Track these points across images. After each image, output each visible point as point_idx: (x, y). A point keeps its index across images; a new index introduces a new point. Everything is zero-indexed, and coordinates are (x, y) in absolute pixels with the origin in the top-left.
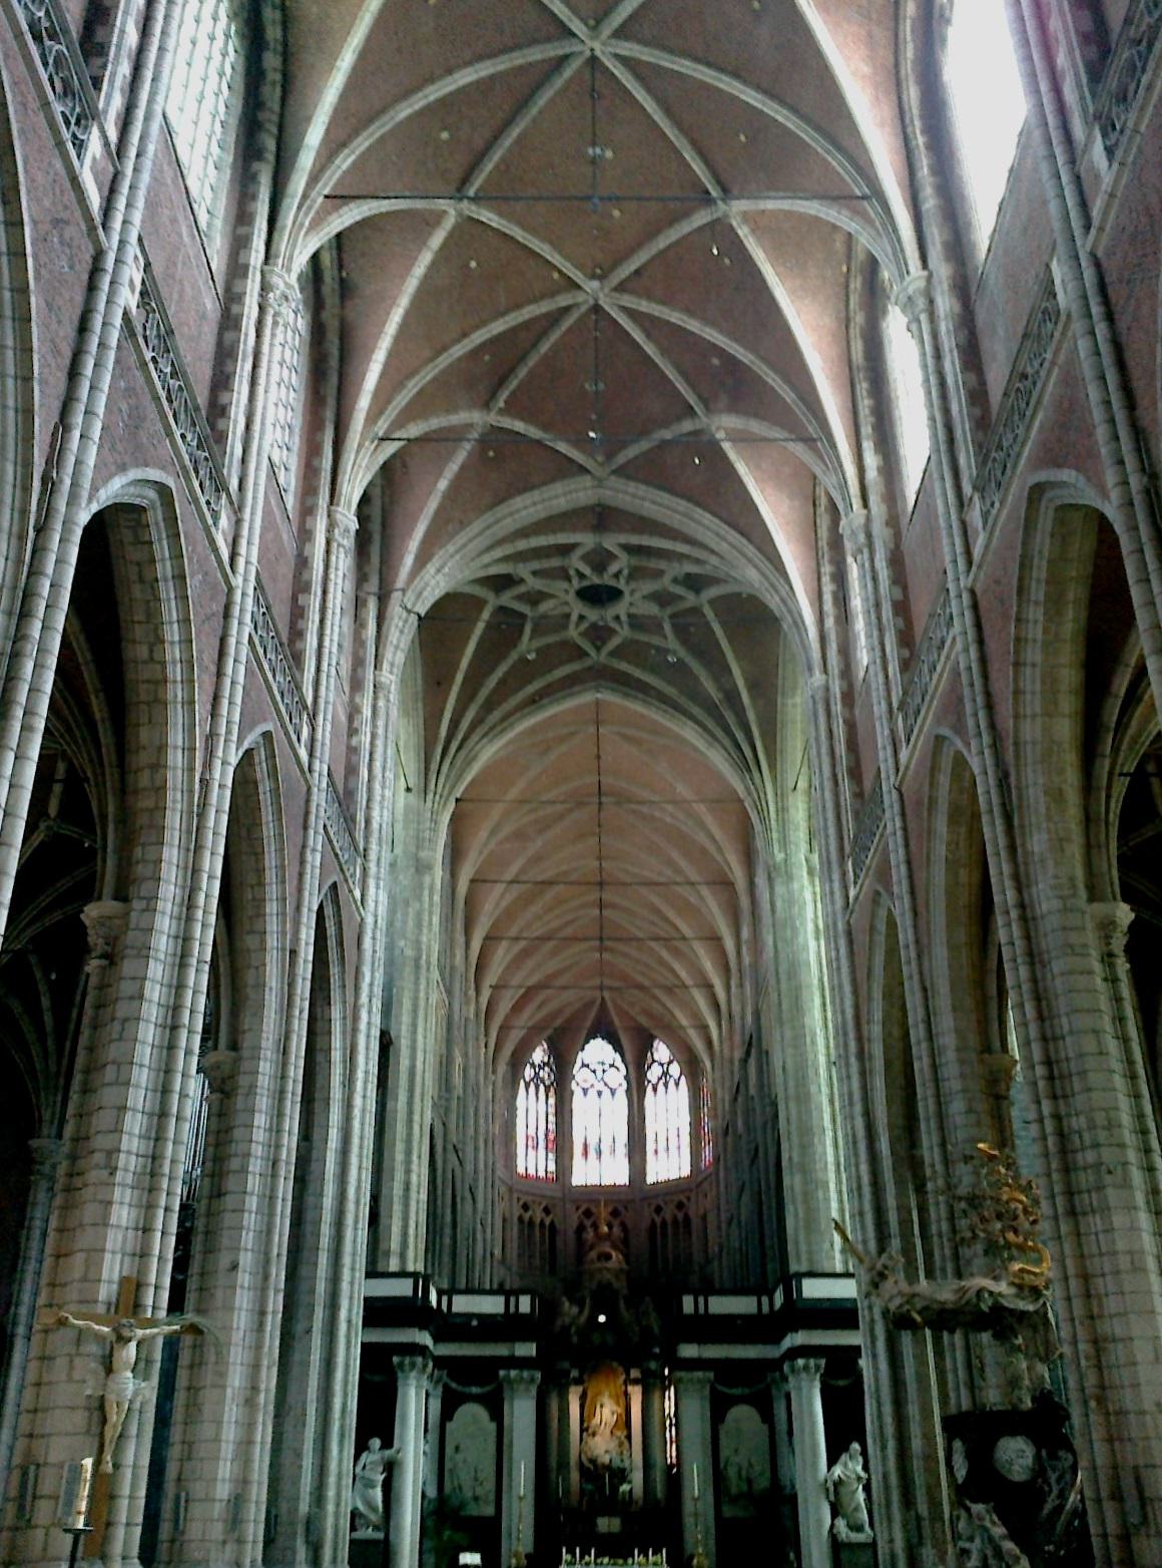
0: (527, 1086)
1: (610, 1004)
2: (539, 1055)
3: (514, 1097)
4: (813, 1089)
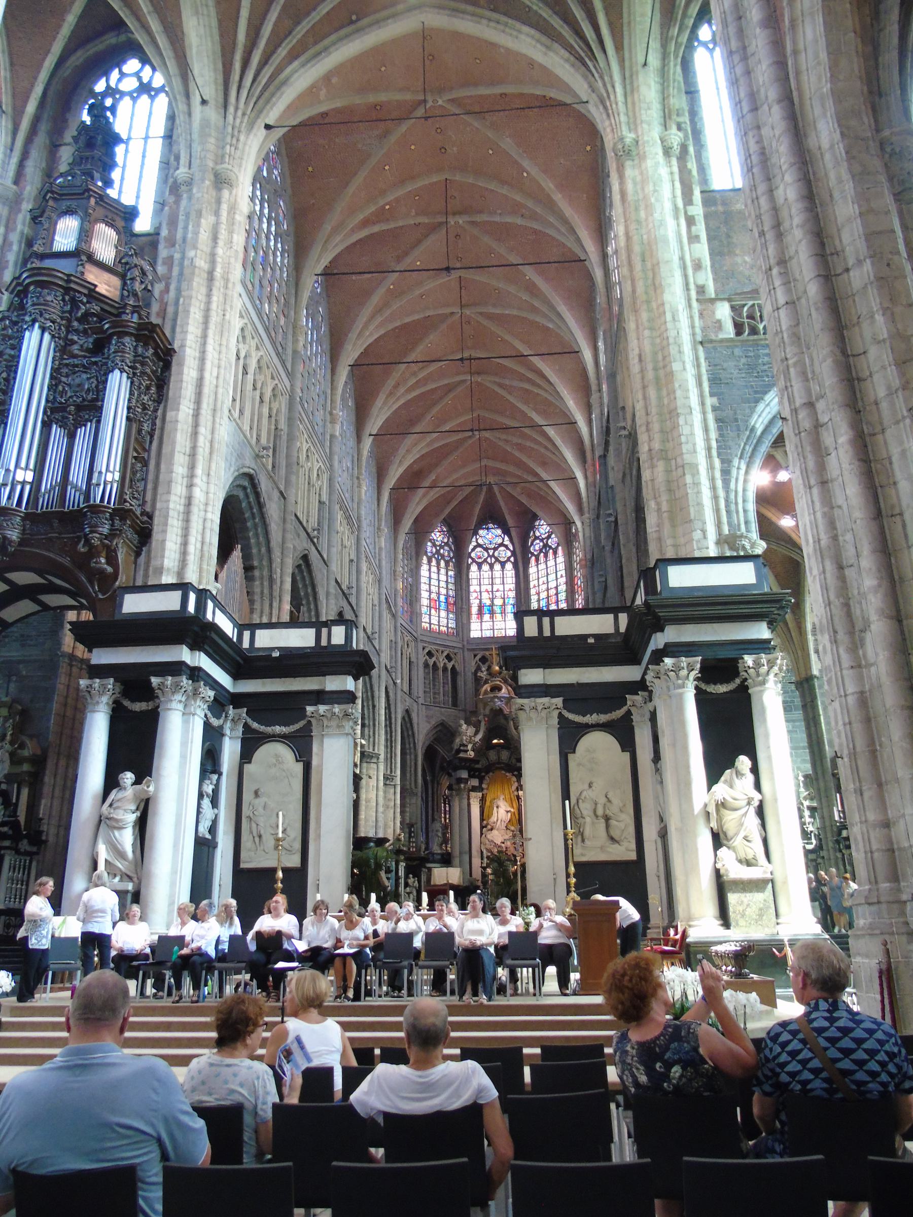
0: (430, 562)
1: (496, 488)
2: (438, 536)
3: (418, 567)
4: (676, 366)
